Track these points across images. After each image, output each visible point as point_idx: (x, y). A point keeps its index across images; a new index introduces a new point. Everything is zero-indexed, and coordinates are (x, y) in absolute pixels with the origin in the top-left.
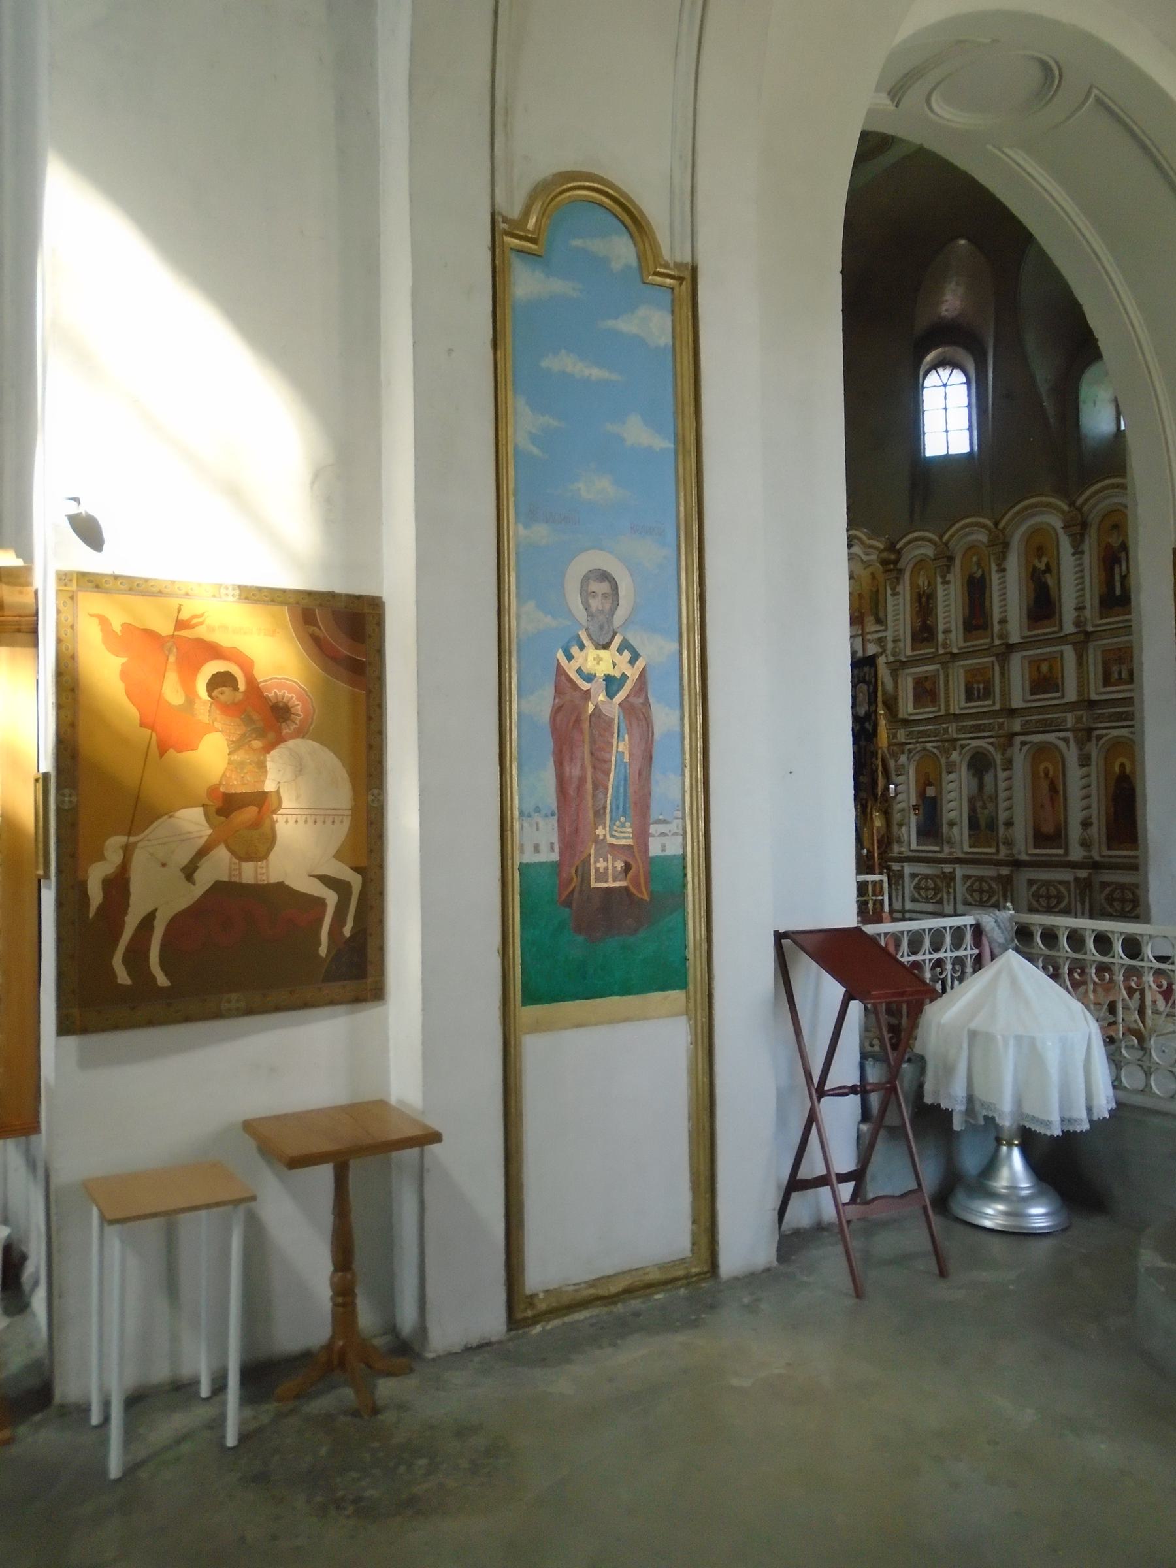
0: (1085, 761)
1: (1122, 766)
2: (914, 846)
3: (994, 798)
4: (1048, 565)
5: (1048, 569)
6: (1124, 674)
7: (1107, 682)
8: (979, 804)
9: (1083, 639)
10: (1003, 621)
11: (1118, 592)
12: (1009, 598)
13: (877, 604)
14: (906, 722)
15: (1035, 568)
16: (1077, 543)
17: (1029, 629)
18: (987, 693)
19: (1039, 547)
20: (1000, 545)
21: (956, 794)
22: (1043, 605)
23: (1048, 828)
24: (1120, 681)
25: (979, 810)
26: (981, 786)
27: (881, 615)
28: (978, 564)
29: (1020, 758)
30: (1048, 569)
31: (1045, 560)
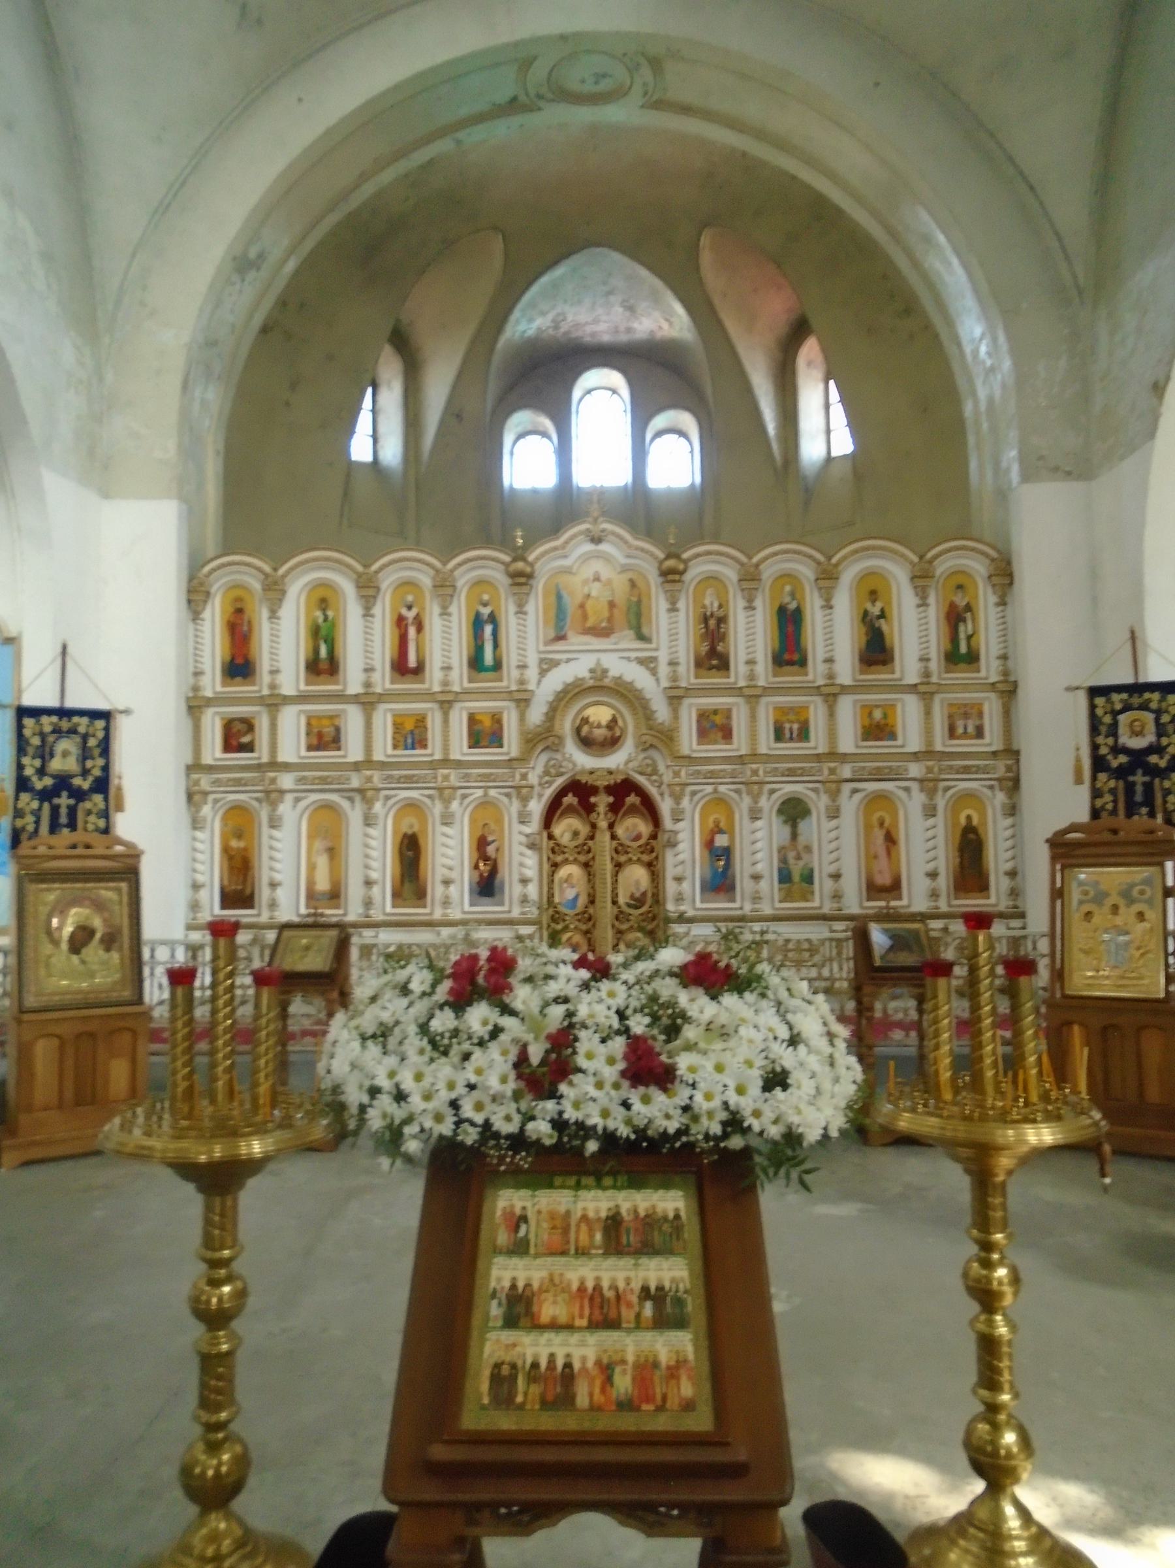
0: (930, 811)
1: (969, 818)
2: (698, 904)
3: (808, 849)
4: (882, 610)
5: (882, 615)
6: (971, 729)
7: (952, 733)
8: (791, 855)
9: (924, 691)
10: (829, 661)
11: (963, 649)
12: (833, 635)
13: (639, 615)
15: (866, 613)
16: (922, 595)
17: (862, 672)
18: (804, 734)
19: (873, 590)
20: (827, 577)
21: (758, 844)
22: (876, 650)
23: (884, 879)
25: (791, 861)
26: (794, 836)
27: (645, 630)
28: (793, 595)
30: (882, 615)
31: (879, 605)
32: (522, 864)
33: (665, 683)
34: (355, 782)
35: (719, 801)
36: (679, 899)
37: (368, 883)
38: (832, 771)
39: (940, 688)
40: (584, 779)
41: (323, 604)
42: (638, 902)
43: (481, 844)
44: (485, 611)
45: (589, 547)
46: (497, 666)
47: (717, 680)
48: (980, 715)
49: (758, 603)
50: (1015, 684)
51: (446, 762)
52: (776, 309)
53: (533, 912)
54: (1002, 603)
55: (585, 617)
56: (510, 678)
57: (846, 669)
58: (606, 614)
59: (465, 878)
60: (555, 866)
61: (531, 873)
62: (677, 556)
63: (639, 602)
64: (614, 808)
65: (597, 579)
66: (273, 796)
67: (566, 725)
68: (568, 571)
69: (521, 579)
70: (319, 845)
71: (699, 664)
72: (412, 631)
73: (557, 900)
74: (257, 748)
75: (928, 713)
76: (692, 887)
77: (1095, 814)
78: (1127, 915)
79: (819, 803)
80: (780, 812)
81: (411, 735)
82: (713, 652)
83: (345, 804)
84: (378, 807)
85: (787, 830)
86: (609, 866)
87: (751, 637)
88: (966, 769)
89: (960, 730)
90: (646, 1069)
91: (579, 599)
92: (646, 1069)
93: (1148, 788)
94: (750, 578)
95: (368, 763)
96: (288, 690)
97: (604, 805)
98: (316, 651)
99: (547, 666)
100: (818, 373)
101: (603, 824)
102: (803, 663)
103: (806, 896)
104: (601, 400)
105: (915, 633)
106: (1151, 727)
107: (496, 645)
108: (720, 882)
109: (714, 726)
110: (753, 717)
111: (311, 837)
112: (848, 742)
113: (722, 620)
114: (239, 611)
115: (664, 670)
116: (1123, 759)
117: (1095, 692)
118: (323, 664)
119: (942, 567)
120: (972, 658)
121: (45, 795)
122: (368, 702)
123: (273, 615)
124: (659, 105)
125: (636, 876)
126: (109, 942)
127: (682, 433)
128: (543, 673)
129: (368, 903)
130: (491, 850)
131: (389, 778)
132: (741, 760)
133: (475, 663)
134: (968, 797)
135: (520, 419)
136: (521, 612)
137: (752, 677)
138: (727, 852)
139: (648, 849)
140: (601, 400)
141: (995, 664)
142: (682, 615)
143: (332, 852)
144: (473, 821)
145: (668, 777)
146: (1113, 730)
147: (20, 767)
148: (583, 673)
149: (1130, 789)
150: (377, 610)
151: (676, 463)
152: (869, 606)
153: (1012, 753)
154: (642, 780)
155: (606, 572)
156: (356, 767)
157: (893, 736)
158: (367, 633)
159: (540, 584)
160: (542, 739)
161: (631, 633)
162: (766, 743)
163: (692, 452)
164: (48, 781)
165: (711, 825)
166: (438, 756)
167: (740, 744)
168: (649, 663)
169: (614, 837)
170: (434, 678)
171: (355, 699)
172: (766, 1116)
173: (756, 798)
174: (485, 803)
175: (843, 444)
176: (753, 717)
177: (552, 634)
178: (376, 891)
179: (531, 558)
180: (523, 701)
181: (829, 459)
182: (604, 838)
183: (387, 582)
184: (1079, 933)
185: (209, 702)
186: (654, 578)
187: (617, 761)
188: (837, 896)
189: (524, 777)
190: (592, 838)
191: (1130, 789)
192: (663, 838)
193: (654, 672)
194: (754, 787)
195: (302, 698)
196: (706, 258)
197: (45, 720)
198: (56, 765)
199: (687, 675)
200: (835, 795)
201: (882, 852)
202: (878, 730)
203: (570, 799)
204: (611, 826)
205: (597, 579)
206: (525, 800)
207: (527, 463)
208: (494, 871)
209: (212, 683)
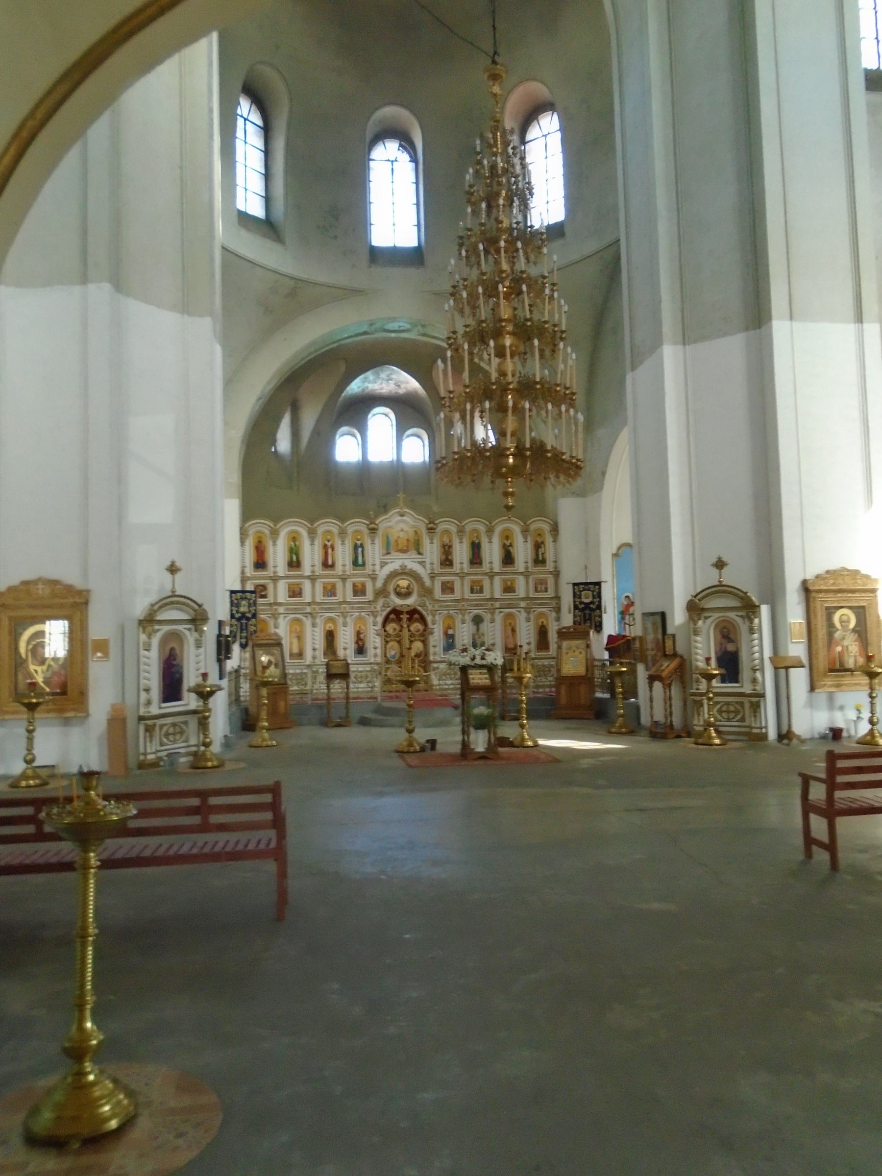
0: (528, 620)
3: (483, 634)
5: (511, 545)
7: (536, 591)
8: (477, 637)
9: (526, 574)
10: (491, 563)
12: (492, 553)
13: (418, 545)
19: (507, 536)
20: (490, 531)
21: (464, 633)
22: (508, 559)
23: (511, 646)
24: (541, 591)
26: (478, 629)
27: (421, 551)
28: (477, 537)
32: (374, 641)
33: (429, 572)
34: (308, 610)
35: (450, 617)
36: (435, 654)
37: (314, 650)
38: (492, 605)
40: (398, 608)
41: (294, 539)
42: (417, 656)
43: (358, 633)
44: (359, 543)
45: (400, 518)
46: (364, 564)
48: (547, 584)
49: (464, 540)
50: (559, 572)
51: (344, 602)
53: (379, 660)
54: (555, 541)
55: (397, 545)
56: (368, 570)
57: (497, 567)
58: (406, 544)
59: (352, 647)
60: (387, 642)
61: (378, 645)
62: (433, 523)
63: (418, 540)
64: (409, 620)
65: (402, 530)
66: (275, 616)
67: (391, 588)
68: (391, 527)
69: (373, 531)
70: (294, 635)
71: (441, 564)
72: (330, 550)
73: (388, 656)
74: (269, 596)
75: (527, 582)
76: (440, 649)
77: (575, 623)
79: (487, 617)
80: (473, 620)
81: (330, 591)
83: (304, 619)
84: (318, 620)
85: (475, 628)
86: (407, 642)
87: (461, 553)
88: (541, 604)
89: (539, 589)
90: (483, 658)
91: (395, 538)
92: (483, 658)
93: (590, 614)
94: (461, 531)
95: (312, 603)
96: (281, 574)
97: (404, 619)
98: (291, 558)
99: (383, 564)
101: (405, 626)
104: (381, 423)
105: (523, 552)
106: (591, 596)
107: (363, 556)
109: (448, 588)
110: (462, 584)
111: (291, 632)
112: (498, 594)
113: (450, 547)
114: (260, 542)
115: (428, 566)
116: (583, 606)
117: (575, 584)
118: (294, 564)
119: (533, 527)
120: (543, 562)
121: (239, 619)
122: (313, 579)
123: (274, 544)
124: (424, 335)
125: (418, 646)
126: (276, 665)
127: (419, 437)
128: (382, 567)
129: (314, 658)
130: (362, 636)
131: (322, 609)
133: (355, 563)
134: (542, 614)
135: (345, 429)
136: (373, 543)
137: (462, 569)
138: (452, 636)
139: (422, 635)
140: (381, 423)
141: (552, 564)
142: (435, 545)
143: (299, 638)
144: (355, 624)
145: (430, 607)
146: (580, 597)
147: (232, 610)
148: (397, 567)
149: (585, 614)
150: (316, 542)
151: (416, 450)
152: (505, 542)
153: (557, 598)
154: (420, 608)
155: (405, 528)
156: (309, 604)
157: (514, 591)
158: (313, 550)
159: (380, 532)
160: (381, 593)
161: (415, 552)
162: (467, 595)
163: (424, 446)
164: (240, 615)
165: (446, 626)
166: (341, 600)
167: (457, 595)
168: (422, 563)
169: (409, 631)
170: (339, 569)
171: (308, 577)
172: (495, 662)
173: (463, 615)
174: (360, 618)
176: (462, 584)
177: (385, 552)
178: (317, 653)
179: (377, 522)
180: (374, 578)
182: (406, 631)
183: (320, 531)
184: (565, 657)
185: (249, 578)
186: (424, 531)
187: (411, 601)
189: (375, 608)
190: (401, 631)
191: (585, 614)
192: (428, 631)
193: (424, 567)
194: (462, 611)
195: (287, 577)
197: (239, 594)
198: (242, 609)
199: (437, 568)
200: (493, 614)
201: (511, 635)
202: (509, 589)
203: (392, 616)
204: (408, 626)
205: (402, 530)
206: (375, 617)
207: (346, 449)
208: (363, 645)
209: (250, 571)
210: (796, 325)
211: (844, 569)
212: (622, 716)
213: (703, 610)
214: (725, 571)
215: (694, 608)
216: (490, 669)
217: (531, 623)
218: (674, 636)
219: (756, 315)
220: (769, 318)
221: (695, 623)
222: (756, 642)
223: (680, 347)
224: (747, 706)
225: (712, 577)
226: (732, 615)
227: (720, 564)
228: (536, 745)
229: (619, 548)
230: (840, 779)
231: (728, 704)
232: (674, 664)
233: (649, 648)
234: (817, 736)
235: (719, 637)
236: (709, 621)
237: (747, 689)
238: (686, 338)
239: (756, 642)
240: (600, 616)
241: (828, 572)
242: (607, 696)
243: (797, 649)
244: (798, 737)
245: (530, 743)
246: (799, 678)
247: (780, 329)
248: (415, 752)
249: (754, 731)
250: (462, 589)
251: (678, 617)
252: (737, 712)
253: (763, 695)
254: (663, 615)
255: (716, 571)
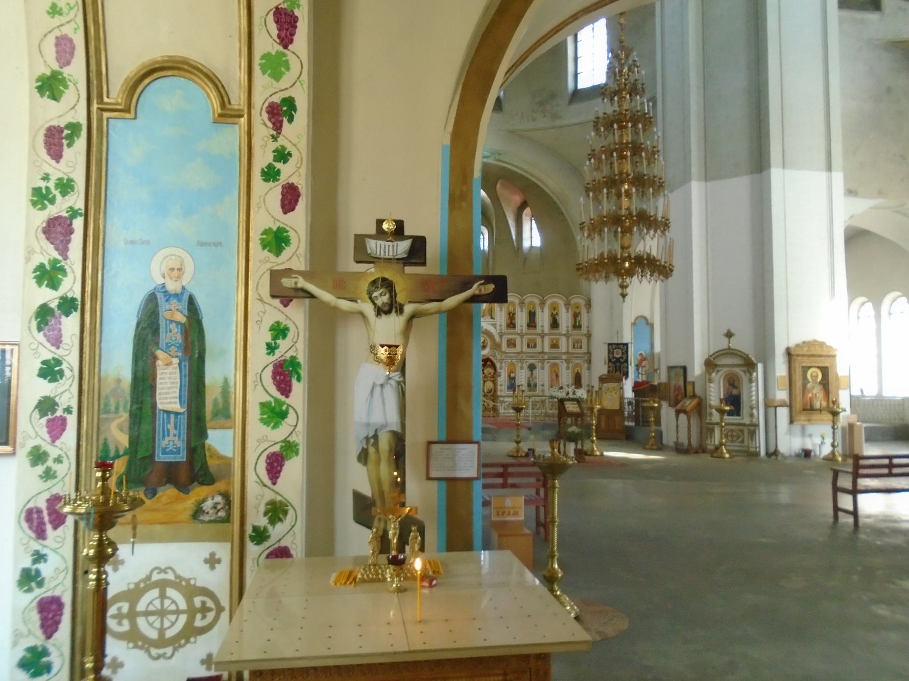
0: (568, 368)
7: (574, 347)
9: (567, 335)
12: (543, 319)
14: (505, 353)
18: (535, 346)
19: (554, 307)
20: (543, 303)
21: (522, 377)
22: (555, 324)
29: (547, 366)
35: (512, 364)
36: (501, 391)
39: (571, 335)
42: (490, 391)
47: (512, 331)
52: (517, 199)
54: (588, 312)
57: (547, 329)
75: (568, 341)
76: (505, 388)
77: (609, 372)
78: (613, 393)
79: (539, 365)
82: (511, 323)
87: (522, 319)
90: (574, 394)
92: (574, 394)
94: (522, 303)
100: (529, 218)
102: (535, 327)
103: (535, 390)
105: (565, 320)
108: (512, 386)
109: (511, 344)
112: (547, 349)
113: (514, 314)
115: (498, 327)
117: (609, 344)
120: (580, 327)
124: (498, 160)
125: (489, 385)
132: (518, 353)
134: (577, 365)
138: (514, 378)
145: (499, 357)
153: (589, 353)
157: (558, 347)
162: (525, 349)
167: (518, 349)
168: (494, 325)
175: (537, 242)
181: (531, 247)
188: (543, 391)
194: (522, 361)
196: (498, 186)
200: (543, 363)
202: (554, 346)
210: (787, 172)
211: (815, 341)
212: (654, 437)
213: (716, 365)
214: (732, 339)
215: (710, 364)
216: (578, 401)
217: (570, 371)
218: (693, 383)
219: (759, 163)
220: (769, 167)
221: (710, 374)
222: (754, 389)
223: (704, 183)
224: (746, 433)
225: (723, 343)
226: (737, 370)
227: (729, 335)
228: (602, 455)
229: (636, 319)
230: (862, 471)
231: (732, 431)
232: (695, 402)
233: (678, 390)
234: (793, 454)
235: (727, 384)
236: (720, 374)
237: (746, 420)
238: (707, 177)
239: (754, 389)
240: (627, 368)
241: (804, 342)
242: (632, 424)
243: (782, 395)
244: (783, 455)
245: (598, 453)
246: (783, 414)
247: (776, 174)
248: (521, 456)
249: (752, 450)
250: (521, 345)
251: (697, 369)
252: (738, 437)
253: (757, 425)
254: (685, 369)
255: (726, 340)
